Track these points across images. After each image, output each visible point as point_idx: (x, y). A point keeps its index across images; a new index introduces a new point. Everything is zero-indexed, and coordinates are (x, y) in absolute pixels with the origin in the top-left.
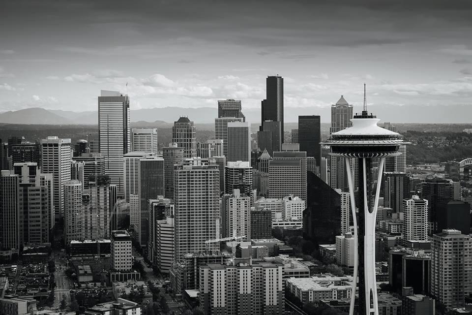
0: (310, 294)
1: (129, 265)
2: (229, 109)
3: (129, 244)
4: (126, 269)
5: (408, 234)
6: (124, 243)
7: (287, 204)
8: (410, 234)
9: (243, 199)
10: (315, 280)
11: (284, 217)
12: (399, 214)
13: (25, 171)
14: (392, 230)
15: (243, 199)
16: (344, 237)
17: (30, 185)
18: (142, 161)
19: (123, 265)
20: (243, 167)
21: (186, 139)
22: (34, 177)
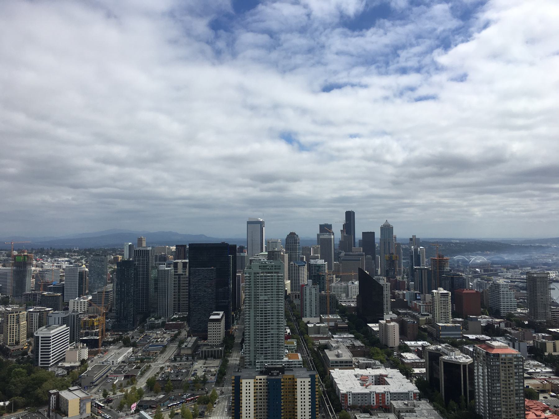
0: (348, 397)
1: (219, 341)
2: (325, 228)
3: (219, 325)
4: (217, 344)
5: (436, 317)
6: (215, 324)
7: (350, 287)
8: (437, 318)
9: (314, 287)
10: (356, 373)
11: (347, 296)
12: (425, 296)
13: (180, 266)
14: (421, 309)
15: (314, 287)
16: (385, 321)
17: (182, 275)
18: (250, 260)
19: (214, 341)
20: (320, 263)
21: (294, 244)
22: (186, 269)
